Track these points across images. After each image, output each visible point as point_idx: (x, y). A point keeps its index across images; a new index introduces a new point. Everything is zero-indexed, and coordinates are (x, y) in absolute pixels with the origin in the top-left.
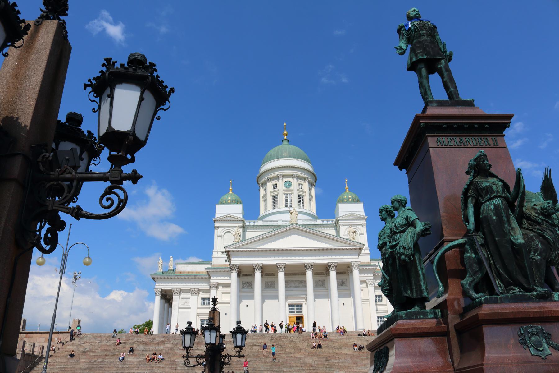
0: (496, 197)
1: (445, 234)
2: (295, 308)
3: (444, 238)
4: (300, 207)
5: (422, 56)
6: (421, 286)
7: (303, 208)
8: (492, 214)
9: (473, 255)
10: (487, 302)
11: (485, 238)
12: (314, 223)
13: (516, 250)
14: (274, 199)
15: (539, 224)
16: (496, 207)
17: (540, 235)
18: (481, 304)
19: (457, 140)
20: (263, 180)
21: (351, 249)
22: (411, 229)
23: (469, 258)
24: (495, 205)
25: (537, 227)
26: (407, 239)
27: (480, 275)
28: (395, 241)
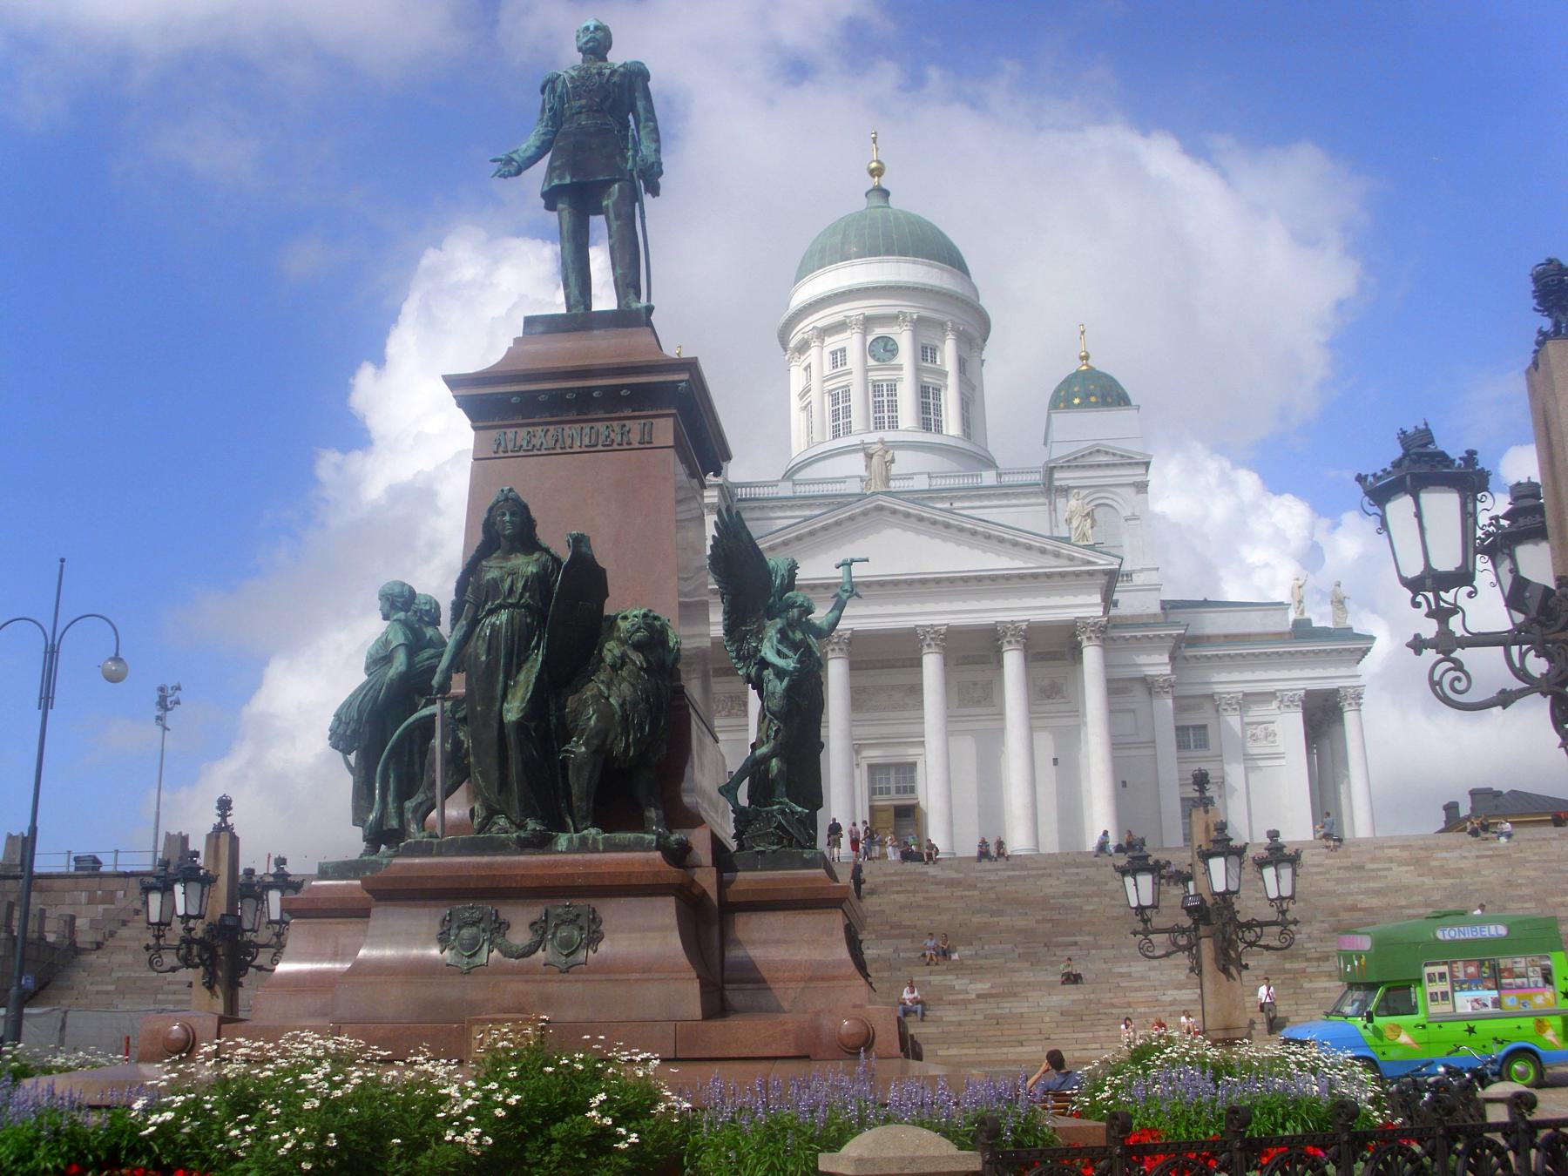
0: (500, 607)
2: (893, 776)
4: (926, 425)
5: (561, 177)
7: (939, 431)
12: (969, 482)
14: (835, 402)
17: (601, 693)
20: (799, 337)
21: (1077, 575)
24: (493, 625)
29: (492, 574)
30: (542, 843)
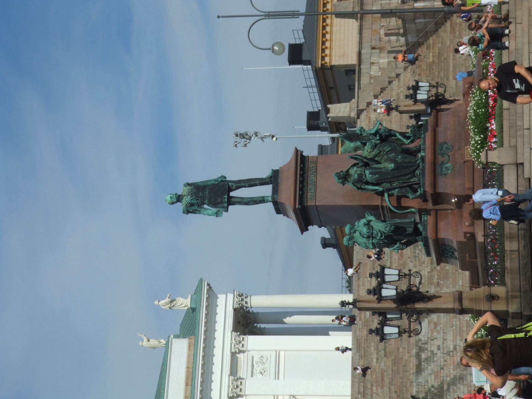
0: (364, 172)
1: (377, 204)
3: (380, 205)
5: (225, 198)
6: (408, 222)
8: (375, 177)
9: (397, 190)
10: (424, 188)
11: (387, 182)
13: (398, 168)
15: (380, 152)
16: (371, 173)
17: (387, 153)
18: (424, 191)
19: (310, 187)
22: (372, 224)
23: (398, 192)
24: (370, 174)
25: (382, 153)
26: (378, 226)
27: (408, 188)
28: (378, 234)
29: (356, 176)
30: (423, 159)
